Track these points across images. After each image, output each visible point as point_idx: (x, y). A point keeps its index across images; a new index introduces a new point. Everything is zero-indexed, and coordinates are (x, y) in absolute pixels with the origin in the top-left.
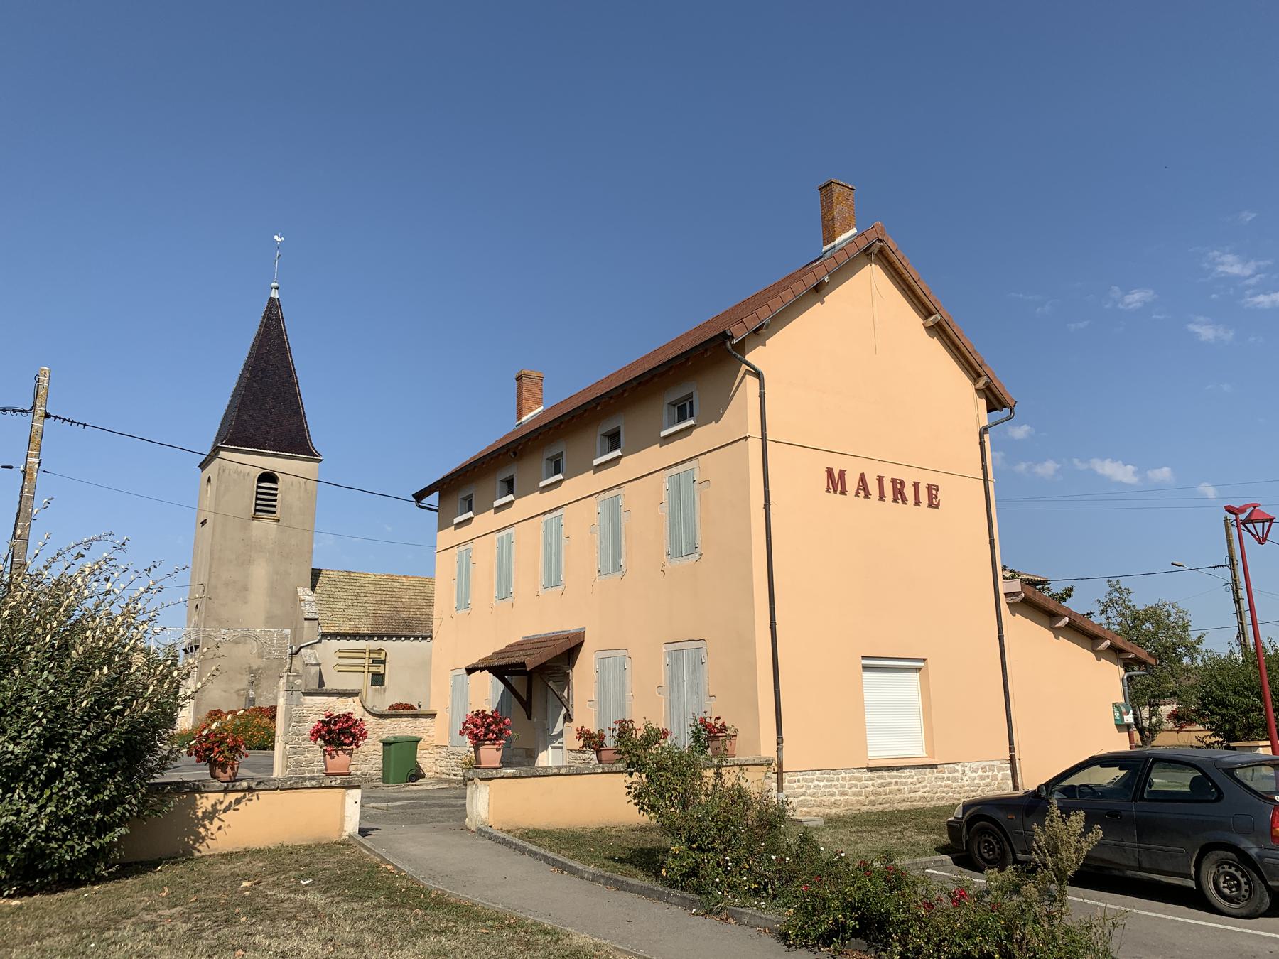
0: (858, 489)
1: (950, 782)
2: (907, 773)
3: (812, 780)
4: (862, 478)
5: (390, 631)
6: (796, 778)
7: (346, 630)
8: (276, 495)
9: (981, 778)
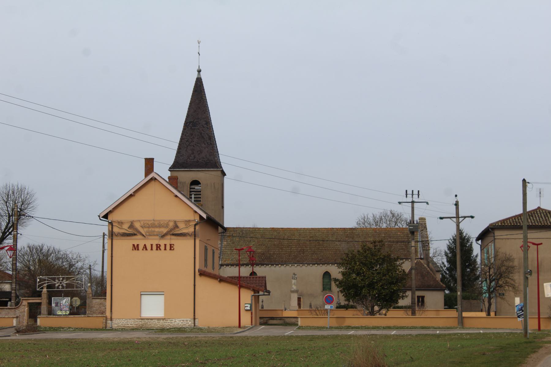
0: (144, 248)
1: (169, 324)
2: (154, 320)
3: (122, 321)
4: (145, 245)
6: (117, 320)
9: (182, 323)
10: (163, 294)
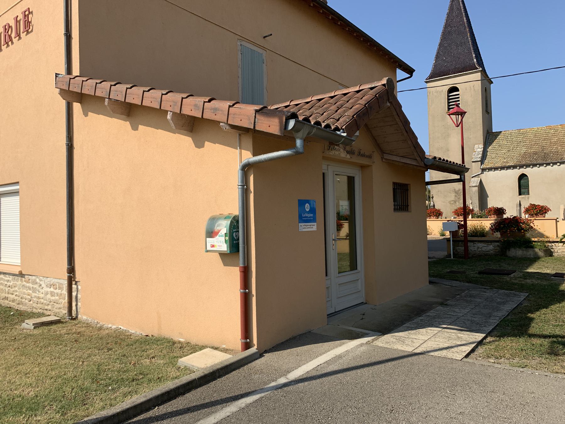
5: (529, 162)
7: (499, 165)
8: (459, 98)
9: (52, 294)
10: (16, 193)
